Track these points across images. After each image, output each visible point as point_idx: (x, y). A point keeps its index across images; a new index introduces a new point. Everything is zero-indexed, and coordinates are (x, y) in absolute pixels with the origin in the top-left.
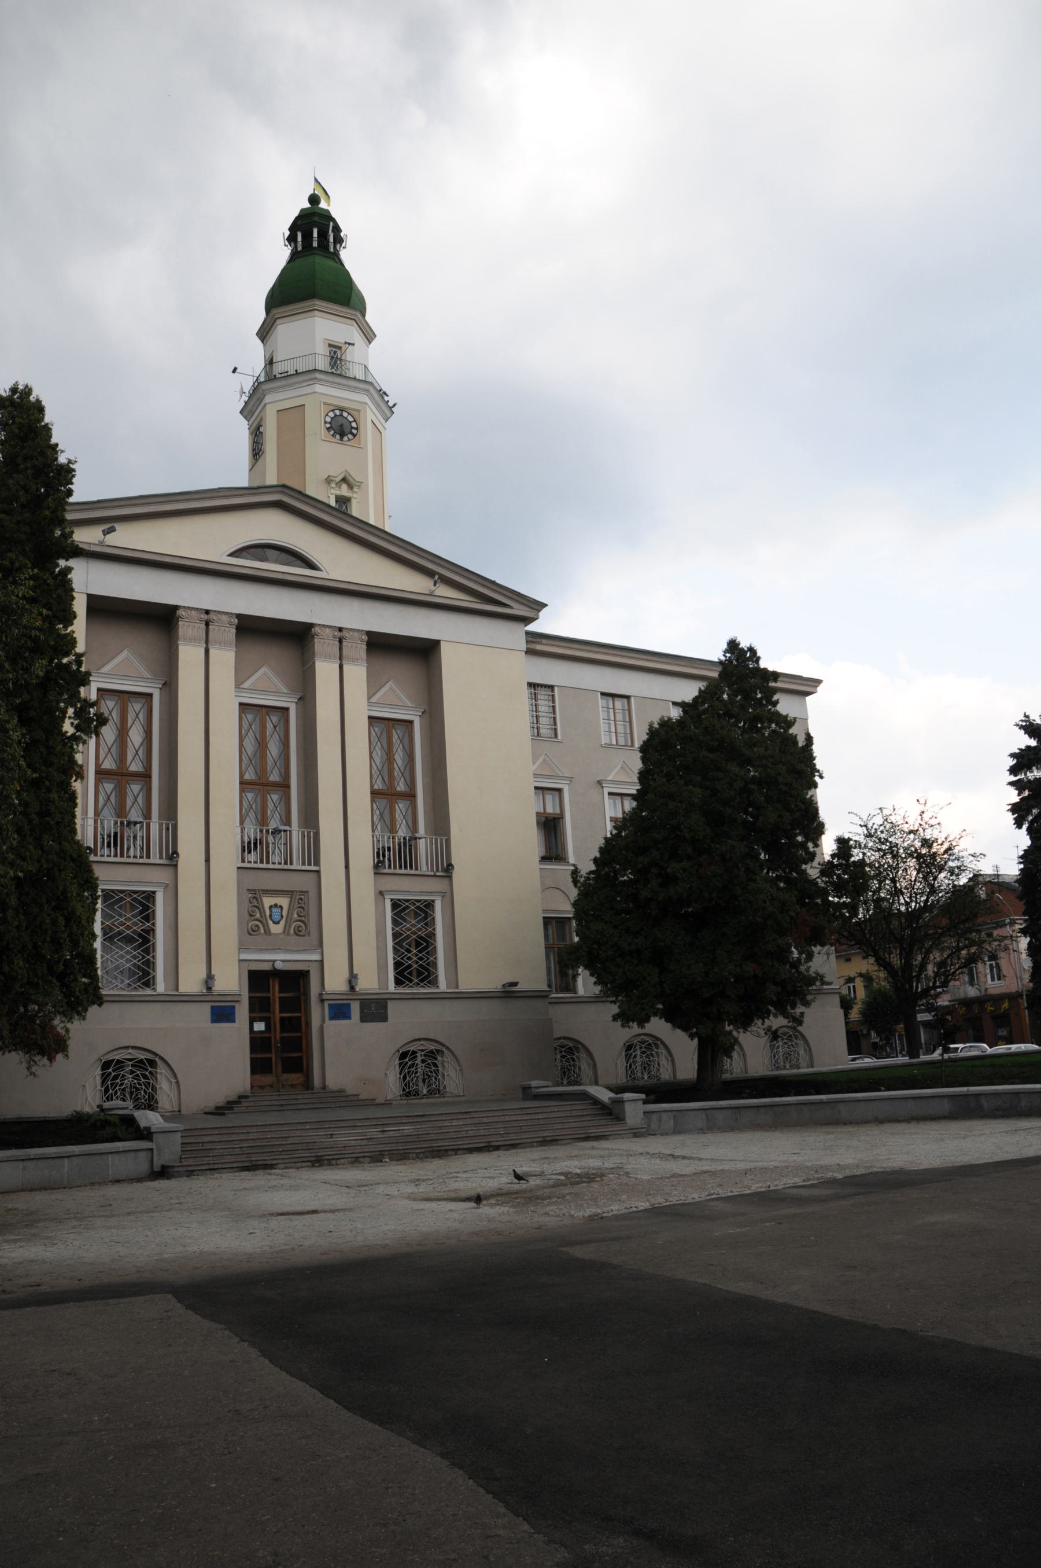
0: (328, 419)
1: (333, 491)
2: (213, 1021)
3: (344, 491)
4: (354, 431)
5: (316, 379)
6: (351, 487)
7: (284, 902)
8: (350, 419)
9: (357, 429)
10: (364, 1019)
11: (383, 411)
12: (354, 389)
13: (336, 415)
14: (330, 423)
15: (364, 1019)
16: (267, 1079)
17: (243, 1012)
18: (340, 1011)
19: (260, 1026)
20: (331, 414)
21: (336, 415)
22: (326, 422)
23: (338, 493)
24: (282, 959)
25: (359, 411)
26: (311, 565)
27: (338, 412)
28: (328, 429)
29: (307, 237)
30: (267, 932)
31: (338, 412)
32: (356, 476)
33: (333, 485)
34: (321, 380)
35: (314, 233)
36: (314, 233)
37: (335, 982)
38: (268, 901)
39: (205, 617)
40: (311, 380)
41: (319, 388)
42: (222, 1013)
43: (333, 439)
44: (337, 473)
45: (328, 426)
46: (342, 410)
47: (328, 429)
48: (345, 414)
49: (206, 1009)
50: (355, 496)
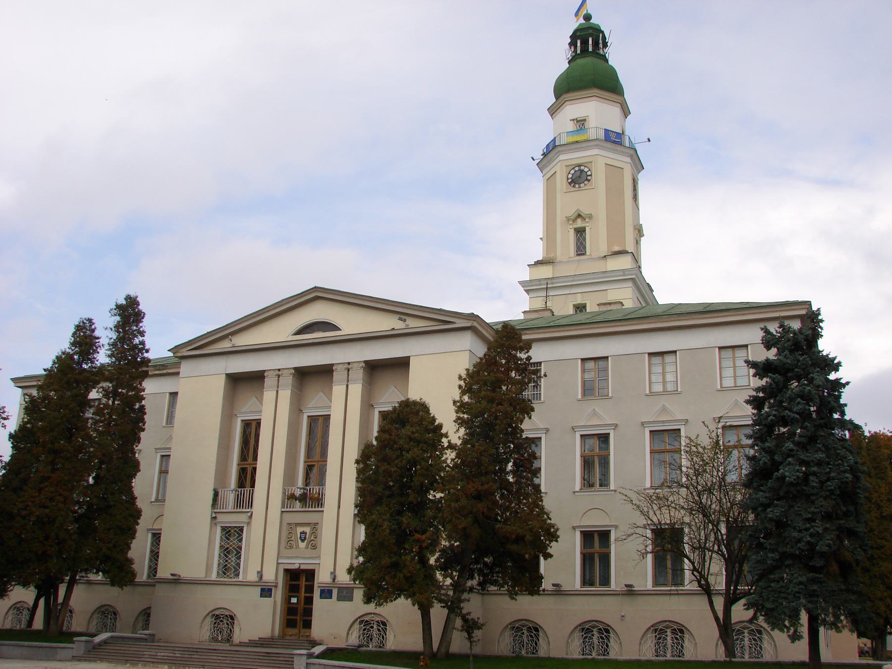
0: (570, 176)
2: (261, 596)
3: (579, 224)
7: (307, 530)
8: (586, 170)
10: (339, 599)
15: (339, 599)
16: (291, 631)
17: (279, 594)
18: (326, 593)
19: (294, 600)
20: (572, 172)
23: (576, 226)
24: (295, 563)
25: (591, 162)
26: (336, 328)
28: (570, 183)
29: (576, 47)
30: (297, 546)
31: (577, 169)
32: (585, 211)
35: (588, 41)
36: (588, 41)
37: (323, 577)
38: (300, 530)
39: (277, 372)
41: (562, 157)
42: (266, 592)
43: (574, 189)
44: (571, 212)
46: (580, 166)
47: (570, 183)
48: (582, 168)
49: (258, 590)
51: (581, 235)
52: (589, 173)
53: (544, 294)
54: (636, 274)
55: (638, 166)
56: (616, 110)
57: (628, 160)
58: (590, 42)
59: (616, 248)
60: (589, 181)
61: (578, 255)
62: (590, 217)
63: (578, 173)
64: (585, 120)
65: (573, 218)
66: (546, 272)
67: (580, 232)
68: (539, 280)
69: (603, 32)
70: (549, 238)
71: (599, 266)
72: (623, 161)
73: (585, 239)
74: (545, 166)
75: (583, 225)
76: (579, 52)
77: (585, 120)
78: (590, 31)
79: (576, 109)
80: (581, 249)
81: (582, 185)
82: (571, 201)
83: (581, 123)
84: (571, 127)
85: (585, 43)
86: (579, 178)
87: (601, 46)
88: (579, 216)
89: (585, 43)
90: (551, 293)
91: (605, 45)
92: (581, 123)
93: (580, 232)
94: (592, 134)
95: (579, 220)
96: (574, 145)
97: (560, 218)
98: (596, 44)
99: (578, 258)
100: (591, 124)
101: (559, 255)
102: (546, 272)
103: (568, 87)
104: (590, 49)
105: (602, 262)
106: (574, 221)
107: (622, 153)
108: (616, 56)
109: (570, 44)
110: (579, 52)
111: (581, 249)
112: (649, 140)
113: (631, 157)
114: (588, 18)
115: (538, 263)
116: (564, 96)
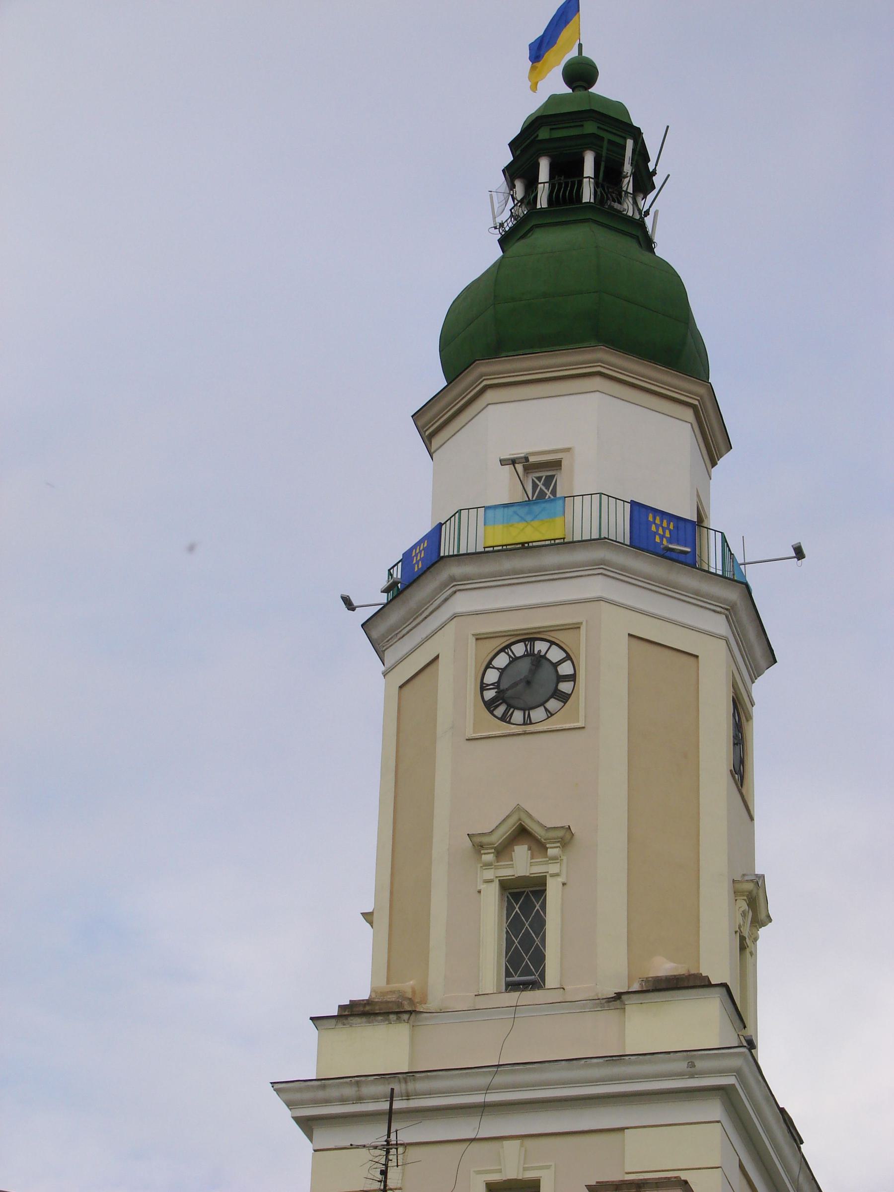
0: (492, 676)
1: (489, 874)
3: (522, 863)
4: (565, 687)
5: (453, 579)
6: (539, 846)
8: (555, 655)
9: (572, 678)
11: (697, 593)
12: (560, 573)
13: (514, 660)
14: (497, 685)
20: (502, 660)
21: (514, 660)
22: (483, 687)
23: (506, 873)
25: (576, 627)
27: (519, 650)
28: (490, 706)
29: (531, 184)
31: (519, 650)
32: (545, 815)
33: (489, 857)
34: (467, 578)
35: (579, 161)
36: (579, 161)
40: (444, 585)
41: (463, 602)
44: (491, 819)
45: (490, 694)
46: (529, 638)
50: (553, 868)
51: (527, 908)
52: (565, 669)
53: (376, 1134)
54: (738, 1073)
55: (755, 650)
56: (678, 433)
57: (719, 624)
58: (589, 169)
59: (665, 967)
60: (564, 698)
61: (512, 987)
62: (566, 838)
63: (524, 666)
64: (556, 465)
65: (497, 838)
66: (383, 1049)
67: (524, 900)
68: (358, 1080)
69: (636, 134)
70: (400, 915)
71: (599, 1035)
72: (702, 630)
73: (540, 924)
74: (396, 634)
75: (537, 870)
76: (542, 202)
77: (556, 465)
78: (590, 128)
79: (520, 419)
80: (524, 965)
81: (538, 714)
82: (494, 775)
83: (541, 475)
84: (504, 487)
85: (567, 171)
86: (527, 684)
87: (628, 184)
88: (522, 833)
89: (567, 171)
90: (406, 1133)
91: (645, 182)
92: (541, 475)
93: (524, 900)
94: (582, 520)
95: (521, 851)
96: (513, 558)
97: (446, 838)
98: (609, 175)
99: (513, 997)
100: (578, 479)
101: (438, 993)
102: (383, 1049)
103: (493, 336)
104: (587, 195)
105: (609, 1017)
106: (503, 850)
107: (699, 599)
108: (682, 226)
109: (511, 173)
110: (542, 202)
111: (524, 965)
112: (799, 553)
113: (729, 612)
114: (581, 74)
115: (353, 1012)
116: (483, 368)
